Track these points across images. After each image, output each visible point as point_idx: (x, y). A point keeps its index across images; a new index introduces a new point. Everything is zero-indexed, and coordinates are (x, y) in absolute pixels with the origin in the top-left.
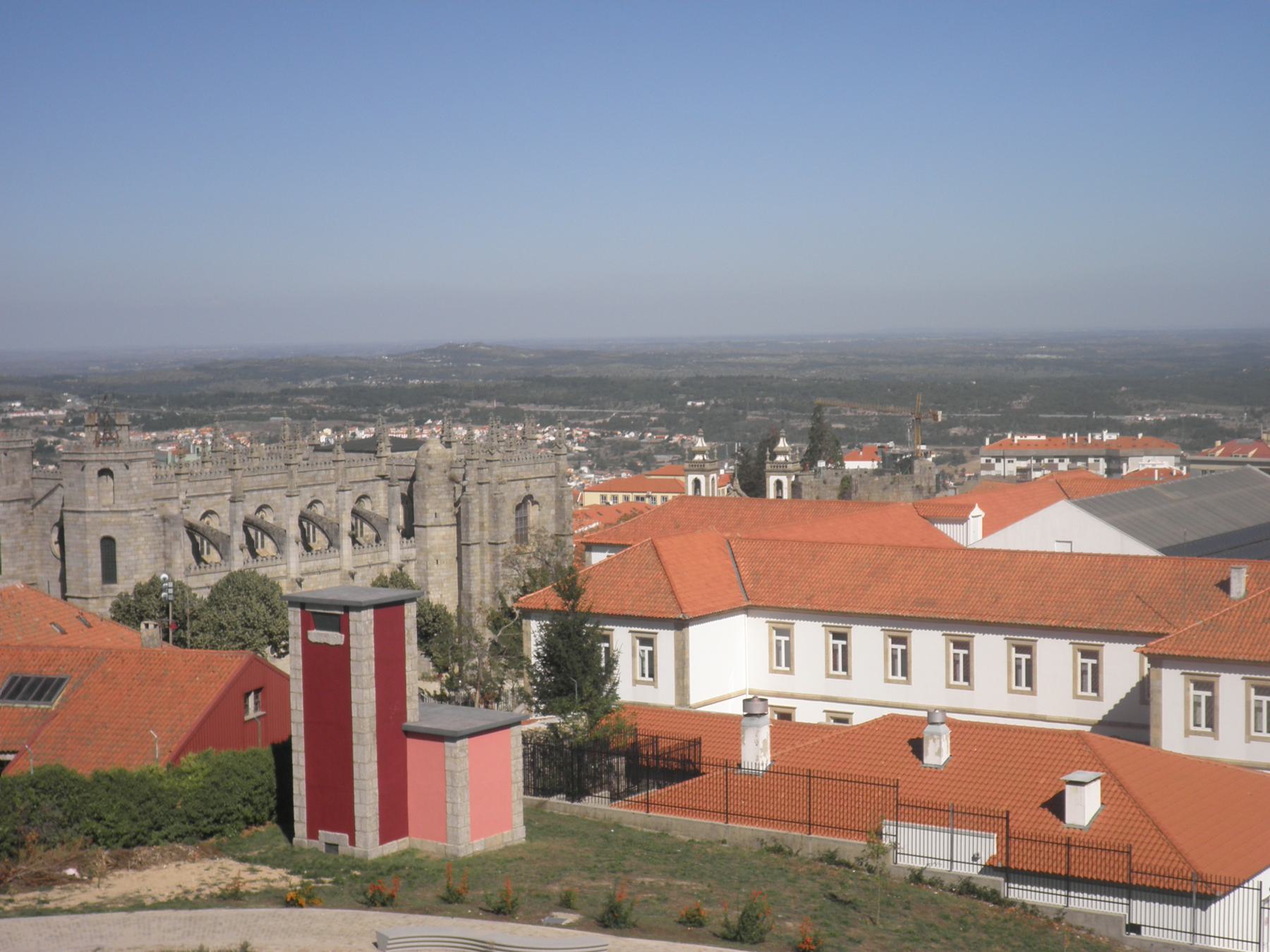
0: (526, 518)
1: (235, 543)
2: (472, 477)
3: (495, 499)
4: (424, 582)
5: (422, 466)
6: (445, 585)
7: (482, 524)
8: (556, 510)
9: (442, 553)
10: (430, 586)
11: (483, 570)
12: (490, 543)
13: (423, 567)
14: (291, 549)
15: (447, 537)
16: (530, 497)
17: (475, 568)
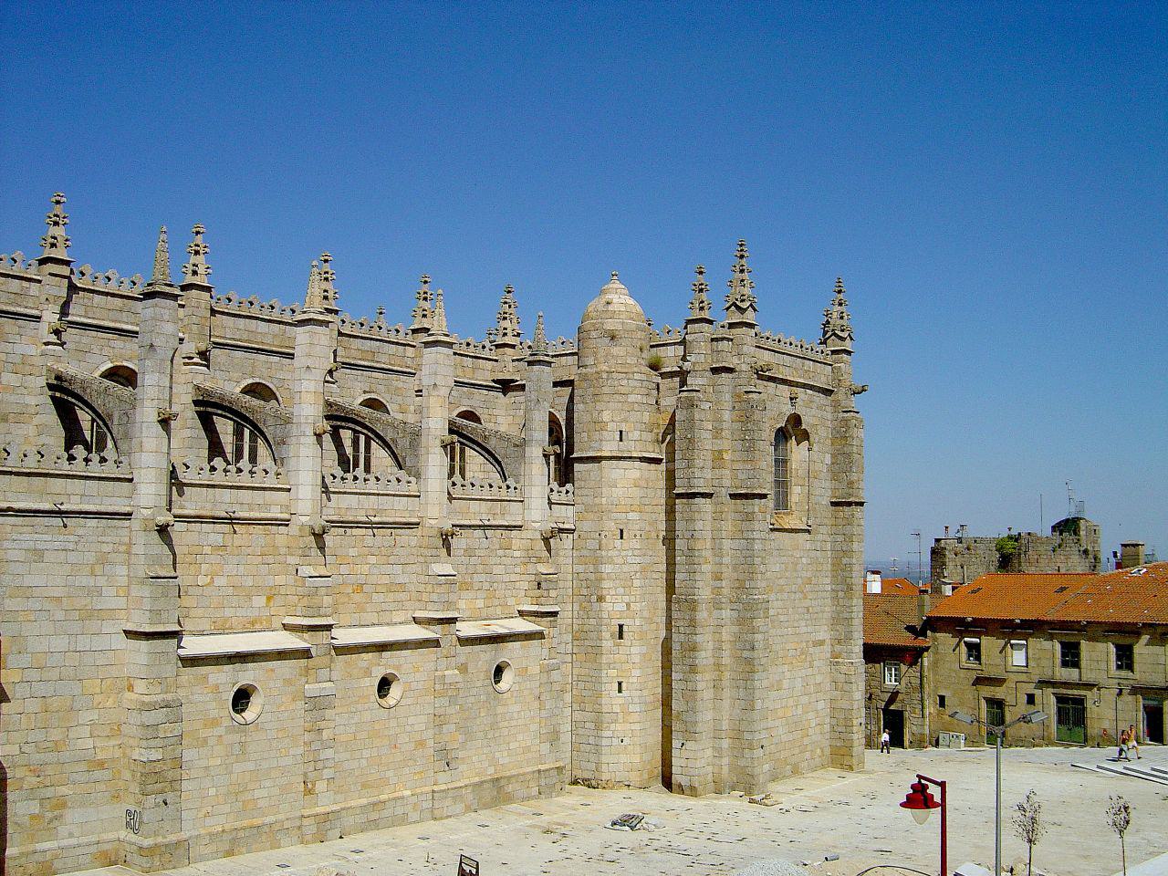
0: (785, 462)
1: (147, 403)
2: (701, 357)
3: (748, 401)
4: (592, 577)
5: (594, 334)
6: (637, 583)
7: (718, 457)
8: (833, 456)
9: (631, 516)
10: (606, 584)
11: (718, 551)
12: (733, 496)
13: (593, 544)
14: (304, 451)
15: (643, 484)
16: (796, 420)
17: (704, 546)
